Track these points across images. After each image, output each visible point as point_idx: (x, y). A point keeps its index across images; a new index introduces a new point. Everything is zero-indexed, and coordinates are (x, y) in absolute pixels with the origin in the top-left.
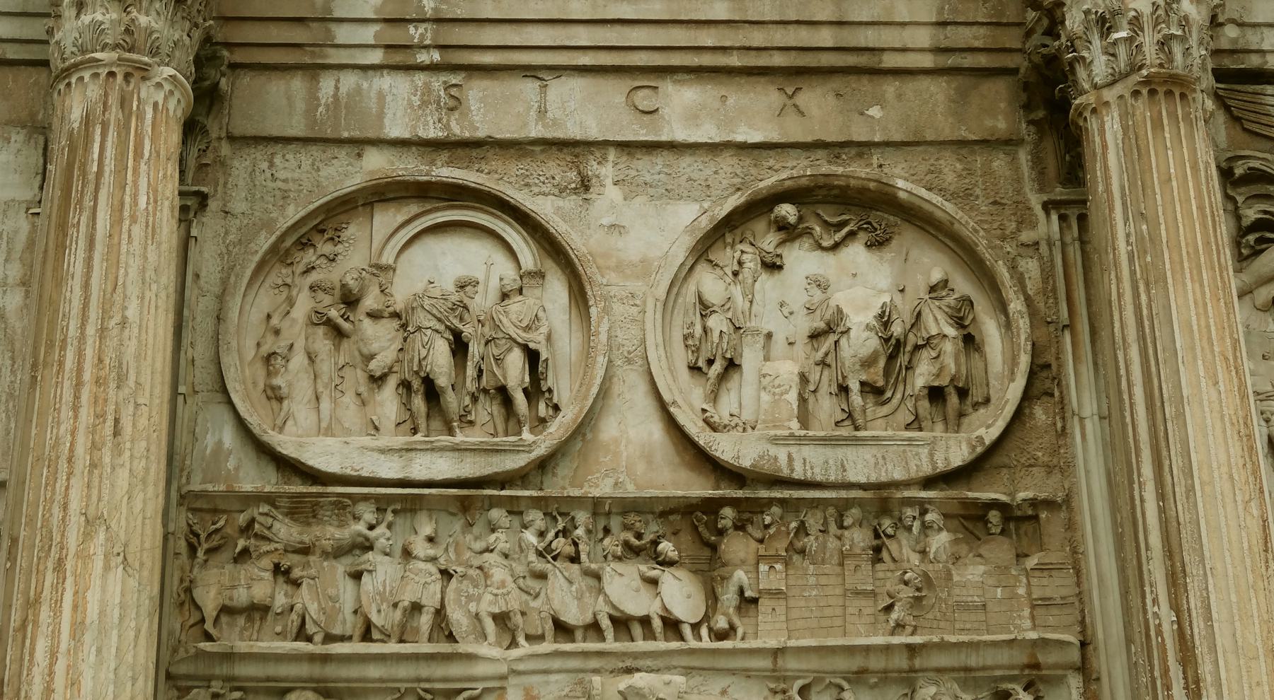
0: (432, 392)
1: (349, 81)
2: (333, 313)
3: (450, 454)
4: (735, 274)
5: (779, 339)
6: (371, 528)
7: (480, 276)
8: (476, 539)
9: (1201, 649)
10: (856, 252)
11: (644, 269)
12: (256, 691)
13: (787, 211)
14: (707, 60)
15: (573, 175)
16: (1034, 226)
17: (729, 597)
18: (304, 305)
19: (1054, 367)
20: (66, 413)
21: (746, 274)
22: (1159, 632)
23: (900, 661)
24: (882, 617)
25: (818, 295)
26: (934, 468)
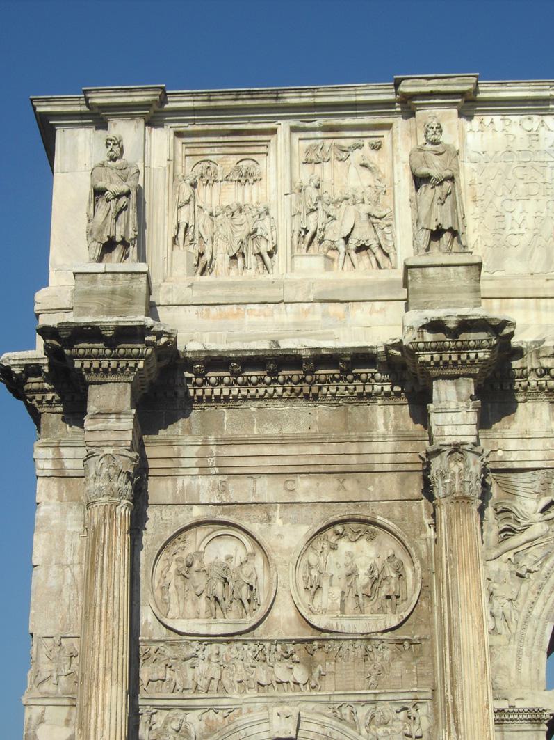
0: (216, 600)
1: (187, 480)
2: (184, 572)
3: (223, 625)
4: (321, 552)
5: (336, 576)
6: (197, 650)
7: (233, 554)
8: (232, 654)
9: (459, 709)
10: (363, 542)
11: (289, 551)
12: (161, 709)
13: (339, 528)
14: (312, 470)
15: (265, 515)
16: (426, 532)
17: (316, 674)
18: (173, 567)
19: (430, 587)
20: (97, 631)
21: (325, 552)
22: (448, 702)
23: (371, 698)
24: (367, 680)
25: (348, 558)
26: (386, 626)
